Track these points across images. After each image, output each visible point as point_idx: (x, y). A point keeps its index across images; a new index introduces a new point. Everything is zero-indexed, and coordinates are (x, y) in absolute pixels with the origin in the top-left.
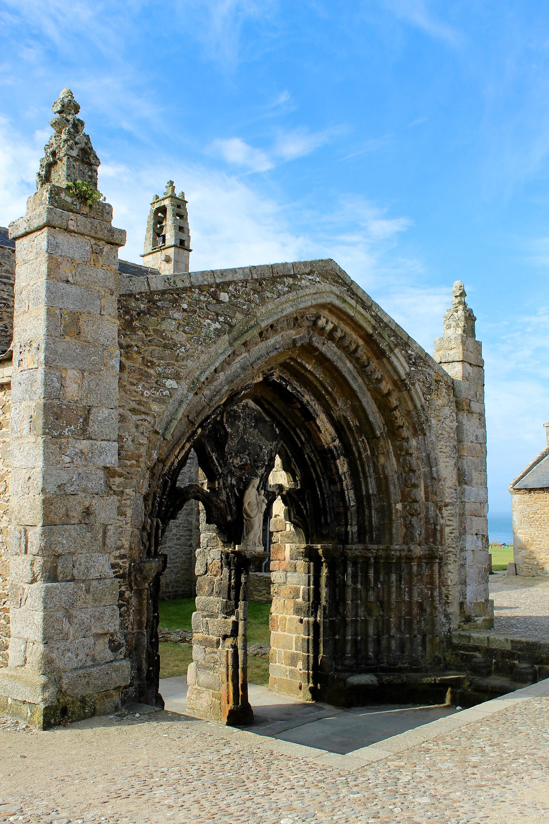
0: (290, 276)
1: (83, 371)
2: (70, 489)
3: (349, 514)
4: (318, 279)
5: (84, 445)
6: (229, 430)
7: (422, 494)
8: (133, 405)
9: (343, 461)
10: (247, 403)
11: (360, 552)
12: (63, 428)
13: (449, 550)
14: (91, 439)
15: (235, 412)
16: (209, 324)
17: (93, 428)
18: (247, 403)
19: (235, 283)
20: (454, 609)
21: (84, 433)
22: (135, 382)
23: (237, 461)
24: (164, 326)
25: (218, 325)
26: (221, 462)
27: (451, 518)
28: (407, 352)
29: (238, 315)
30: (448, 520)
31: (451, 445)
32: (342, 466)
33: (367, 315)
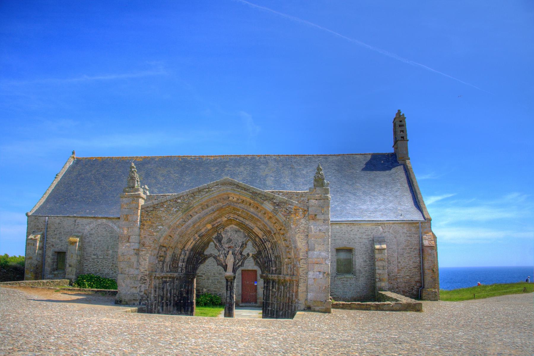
5: (128, 244)
6: (224, 236)
17: (131, 240)
21: (128, 241)
23: (227, 246)
32: (268, 245)
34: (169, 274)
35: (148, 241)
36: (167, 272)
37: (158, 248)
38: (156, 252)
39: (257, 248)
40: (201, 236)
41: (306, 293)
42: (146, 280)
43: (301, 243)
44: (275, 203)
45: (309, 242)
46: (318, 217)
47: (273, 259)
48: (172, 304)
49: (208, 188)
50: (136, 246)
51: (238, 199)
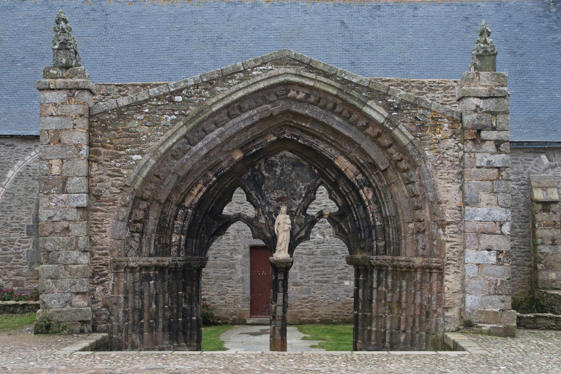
0: (241, 72)
1: (62, 160)
2: (55, 219)
3: (373, 231)
4: (270, 67)
5: (63, 196)
6: (266, 175)
7: (427, 214)
8: (110, 172)
9: (367, 190)
10: (285, 155)
11: (381, 262)
12: (50, 189)
13: (448, 262)
14: (67, 193)
15: (273, 161)
16: (166, 118)
17: (69, 188)
18: (285, 155)
19: (187, 88)
20: (453, 313)
21: (63, 191)
22: (108, 159)
23: (274, 195)
24: (129, 125)
25: (174, 117)
26: (260, 197)
27: (454, 235)
28: (386, 101)
29: (191, 107)
30: (450, 237)
31: (456, 171)
33: (333, 83)
34: (154, 260)
35: (109, 186)
36: (151, 255)
37: (131, 205)
38: (125, 212)
39: (339, 200)
40: (220, 178)
41: (461, 296)
42: (105, 275)
43: (448, 193)
44: (390, 105)
45: (466, 186)
46: (484, 134)
47: (378, 223)
48: (161, 326)
49: (244, 71)
50: (83, 201)
51: (308, 96)
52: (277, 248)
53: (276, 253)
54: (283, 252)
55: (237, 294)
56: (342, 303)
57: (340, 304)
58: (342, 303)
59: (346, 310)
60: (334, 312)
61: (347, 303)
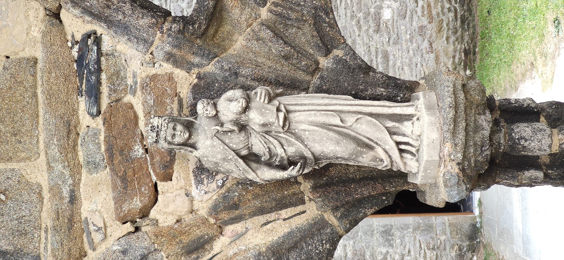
52: (384, 165)
53: (410, 165)
54: (406, 127)
55: (418, 245)
56: (430, 23)
57: (431, 29)
58: (430, 23)
59: (444, 14)
60: (448, 39)
61: (430, 12)
